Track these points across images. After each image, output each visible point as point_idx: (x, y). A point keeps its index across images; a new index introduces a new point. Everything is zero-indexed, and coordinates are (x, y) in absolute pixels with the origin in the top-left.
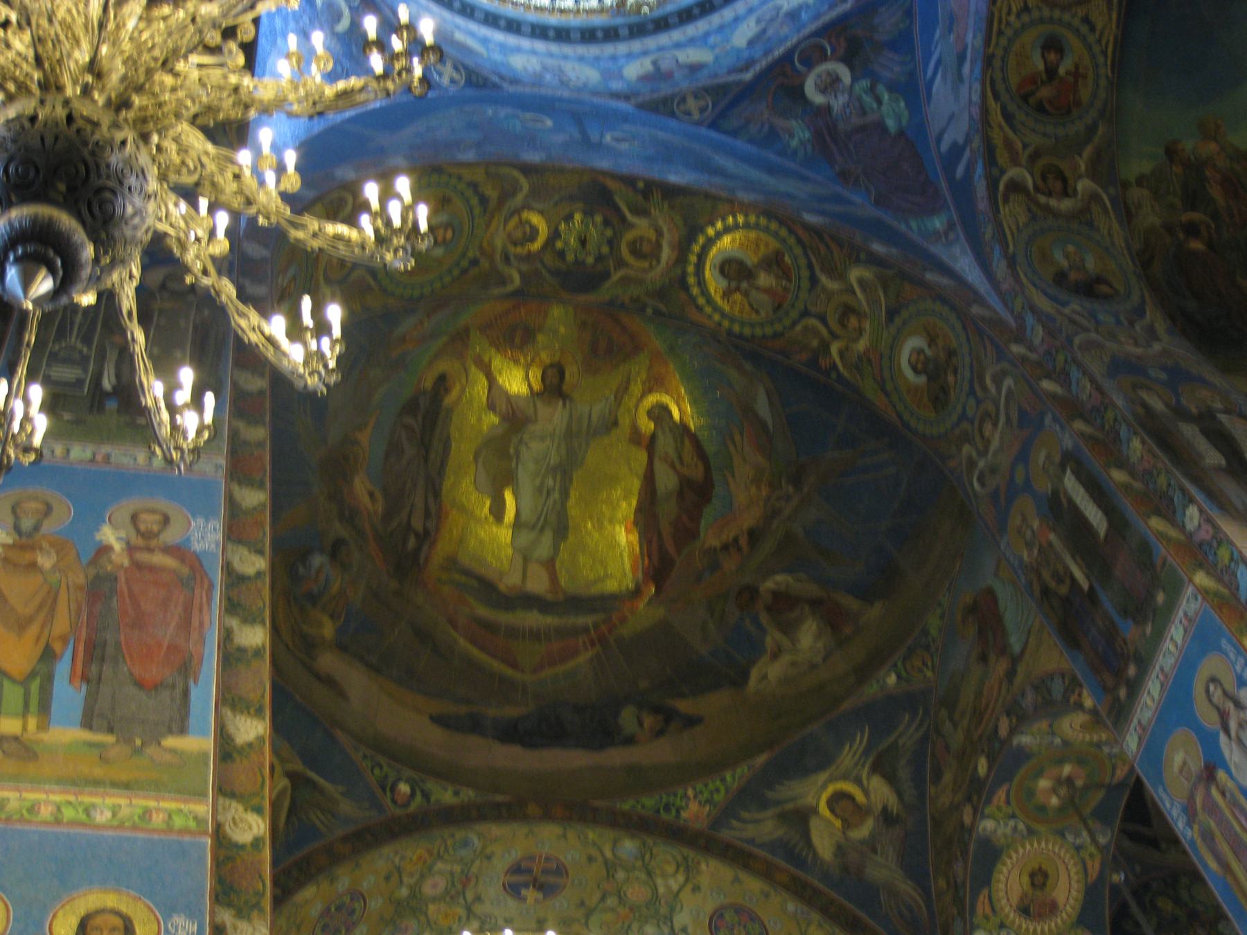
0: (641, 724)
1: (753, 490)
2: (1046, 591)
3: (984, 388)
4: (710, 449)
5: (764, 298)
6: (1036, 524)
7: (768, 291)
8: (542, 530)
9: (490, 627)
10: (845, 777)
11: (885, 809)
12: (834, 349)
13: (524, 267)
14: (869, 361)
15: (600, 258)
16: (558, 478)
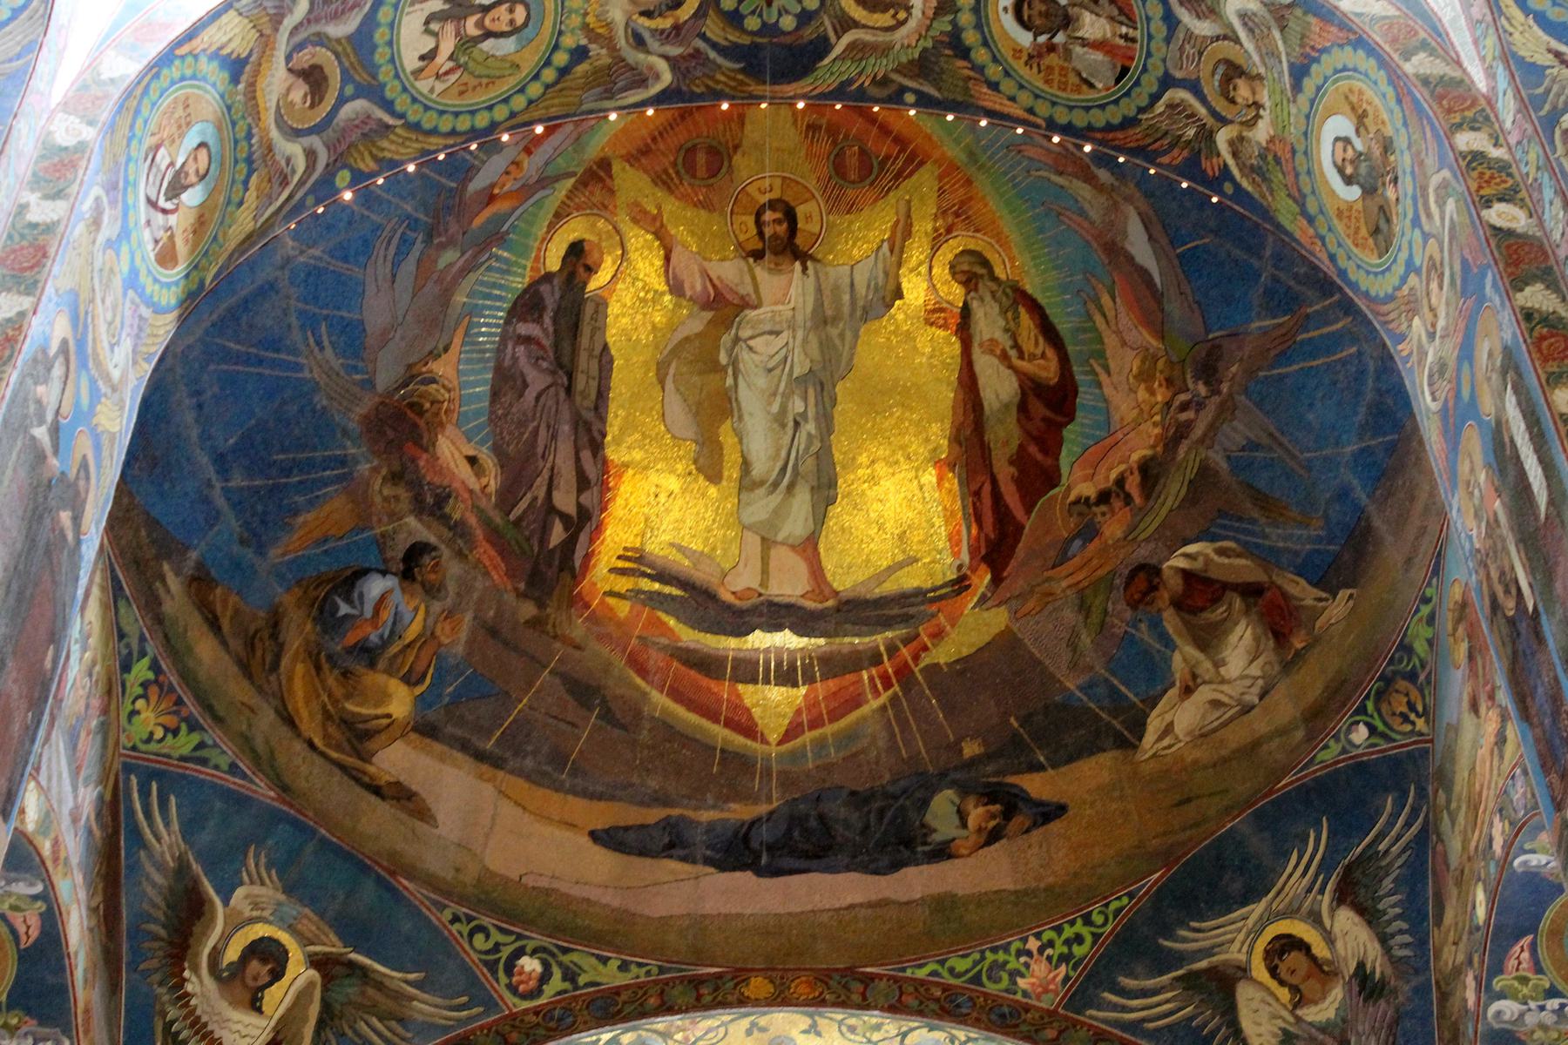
0: (964, 825)
1: (1142, 394)
2: (1495, 606)
3: (1429, 215)
4: (1063, 326)
5: (1098, 56)
6: (1482, 477)
7: (1098, 45)
8: (791, 487)
9: (709, 665)
10: (1290, 913)
11: (1361, 971)
12: (1222, 138)
13: (675, 51)
14: (1277, 160)
15: (805, 17)
16: (811, 392)
